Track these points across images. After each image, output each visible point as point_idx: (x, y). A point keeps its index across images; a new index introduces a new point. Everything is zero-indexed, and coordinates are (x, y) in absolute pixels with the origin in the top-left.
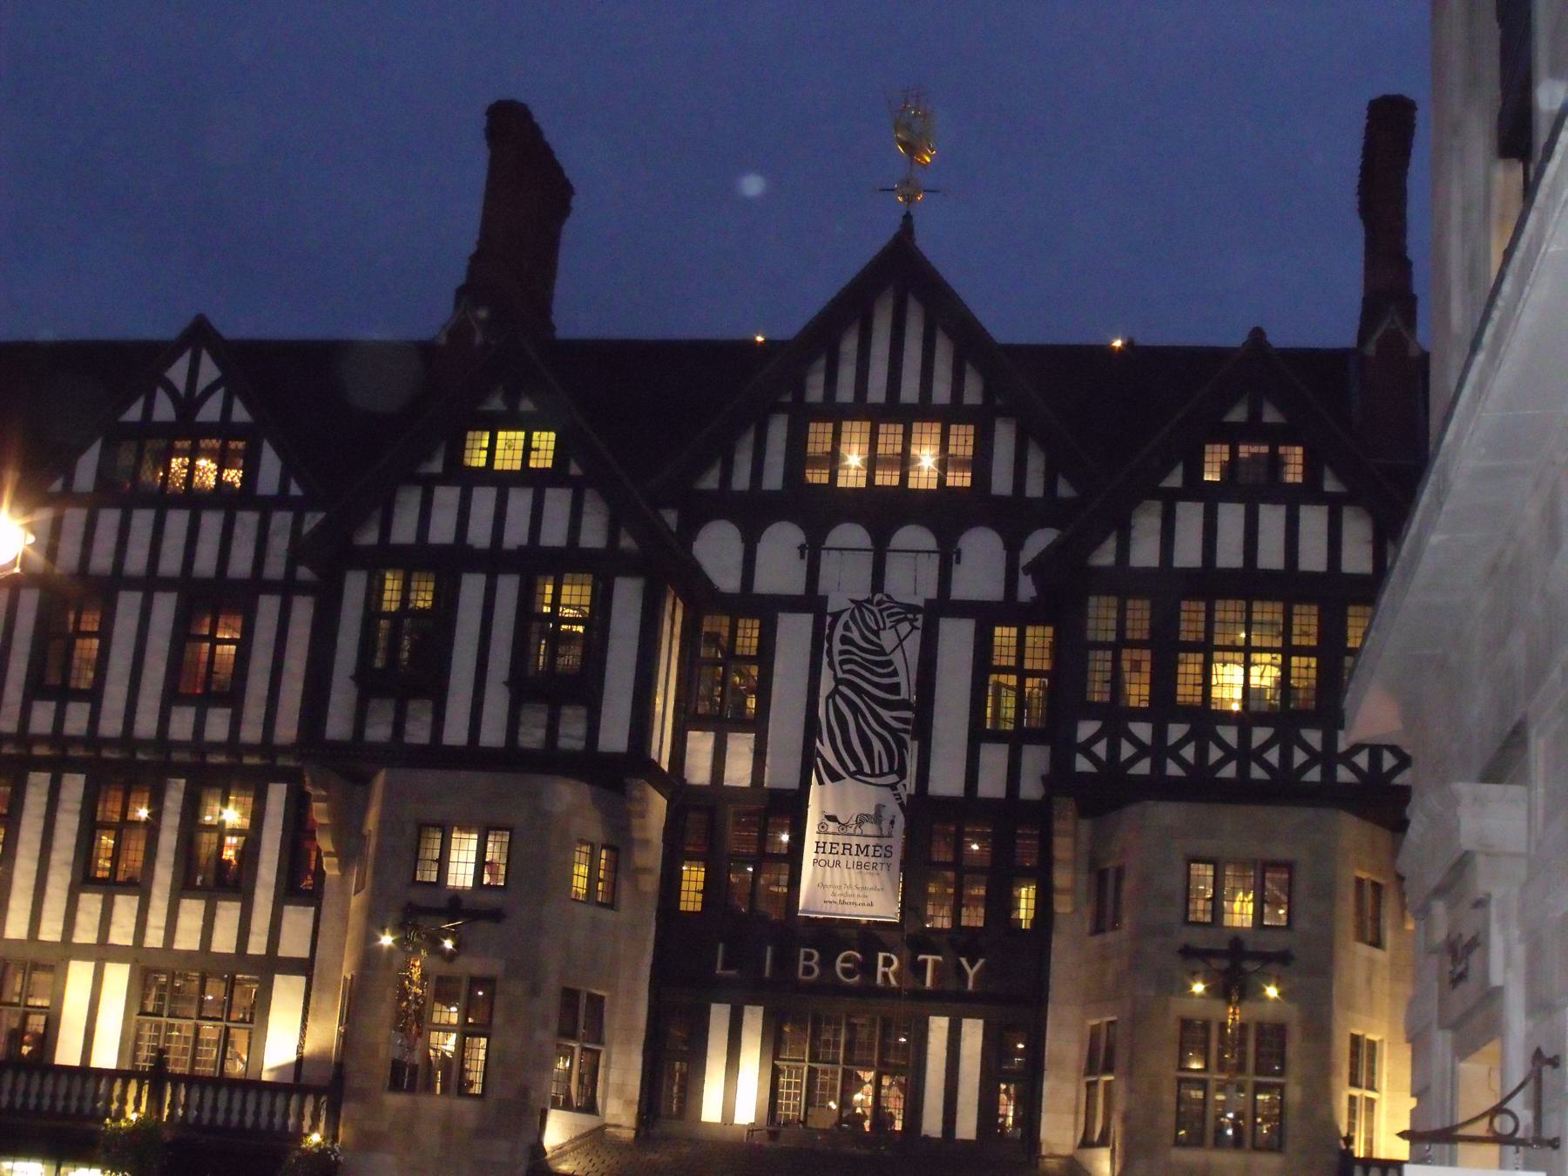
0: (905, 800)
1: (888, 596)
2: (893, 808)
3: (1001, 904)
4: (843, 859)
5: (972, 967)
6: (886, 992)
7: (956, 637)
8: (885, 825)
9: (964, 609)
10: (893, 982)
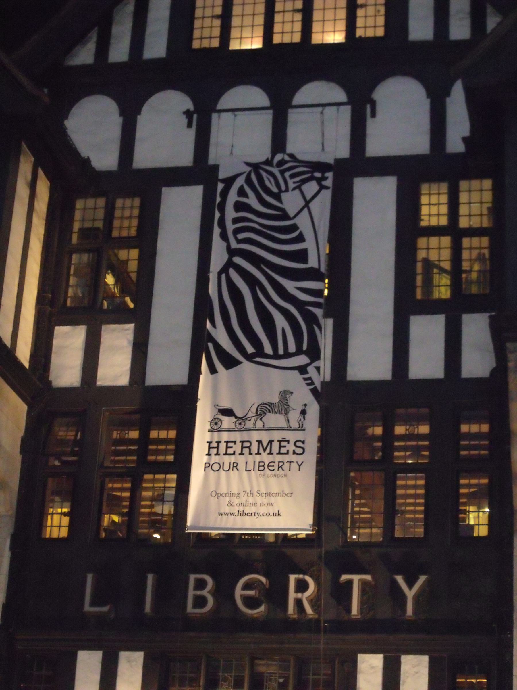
0: (318, 385)
1: (291, 156)
2: (302, 396)
3: (444, 508)
4: (241, 460)
5: (410, 586)
6: (299, 625)
7: (375, 202)
8: (294, 416)
9: (382, 166)
10: (309, 610)
